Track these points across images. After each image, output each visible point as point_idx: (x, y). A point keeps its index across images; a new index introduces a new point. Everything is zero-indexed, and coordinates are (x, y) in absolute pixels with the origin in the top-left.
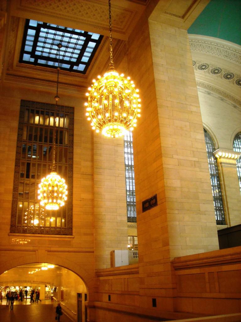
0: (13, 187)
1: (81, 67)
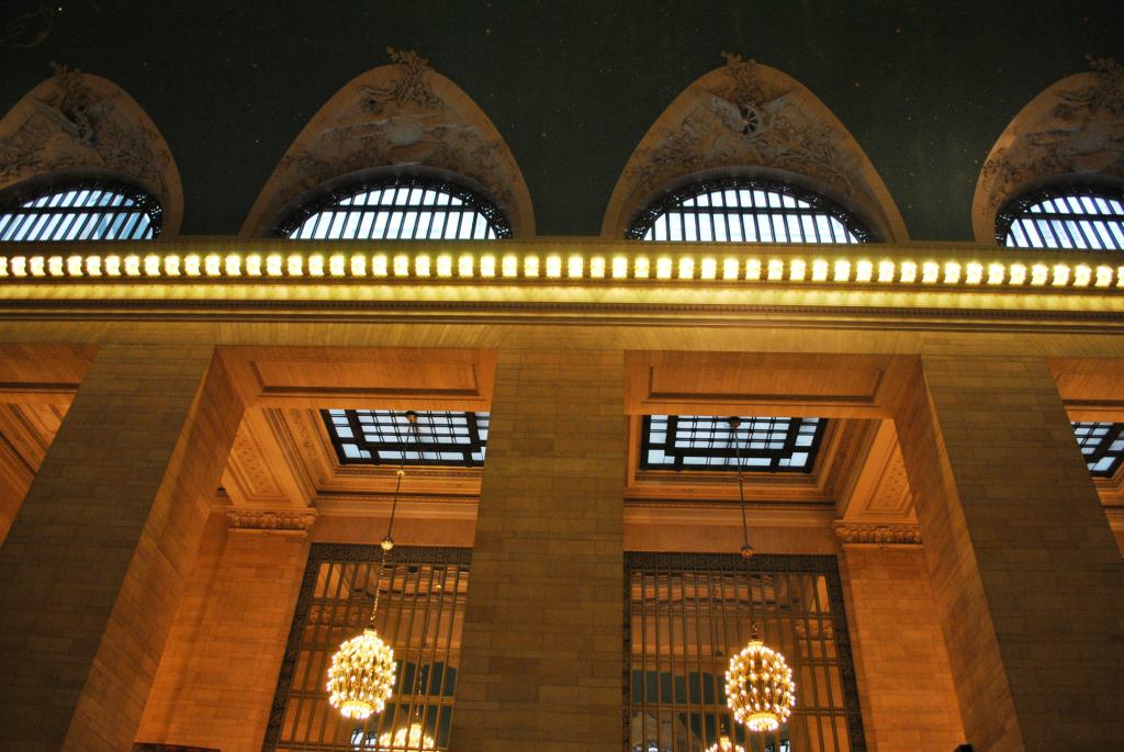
1: (799, 459)
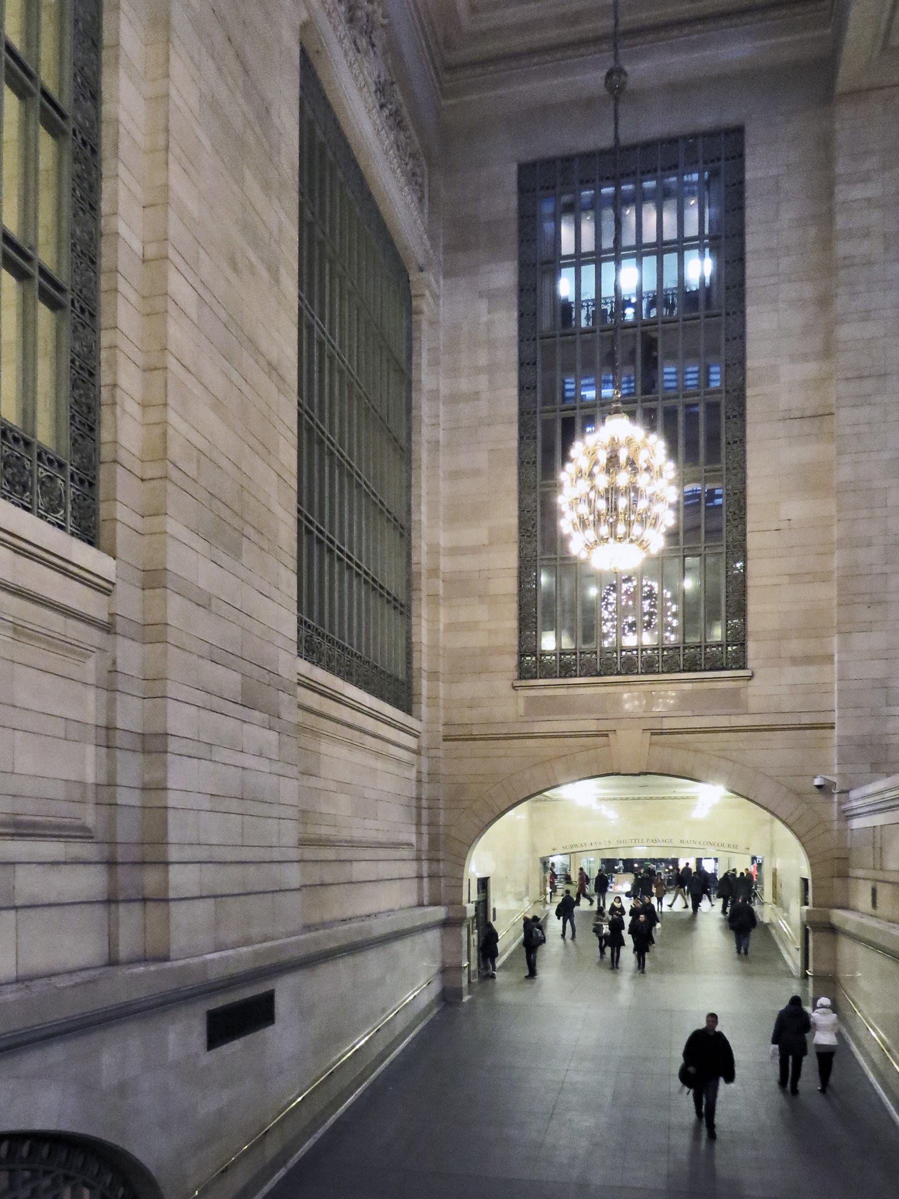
0: (520, 517)
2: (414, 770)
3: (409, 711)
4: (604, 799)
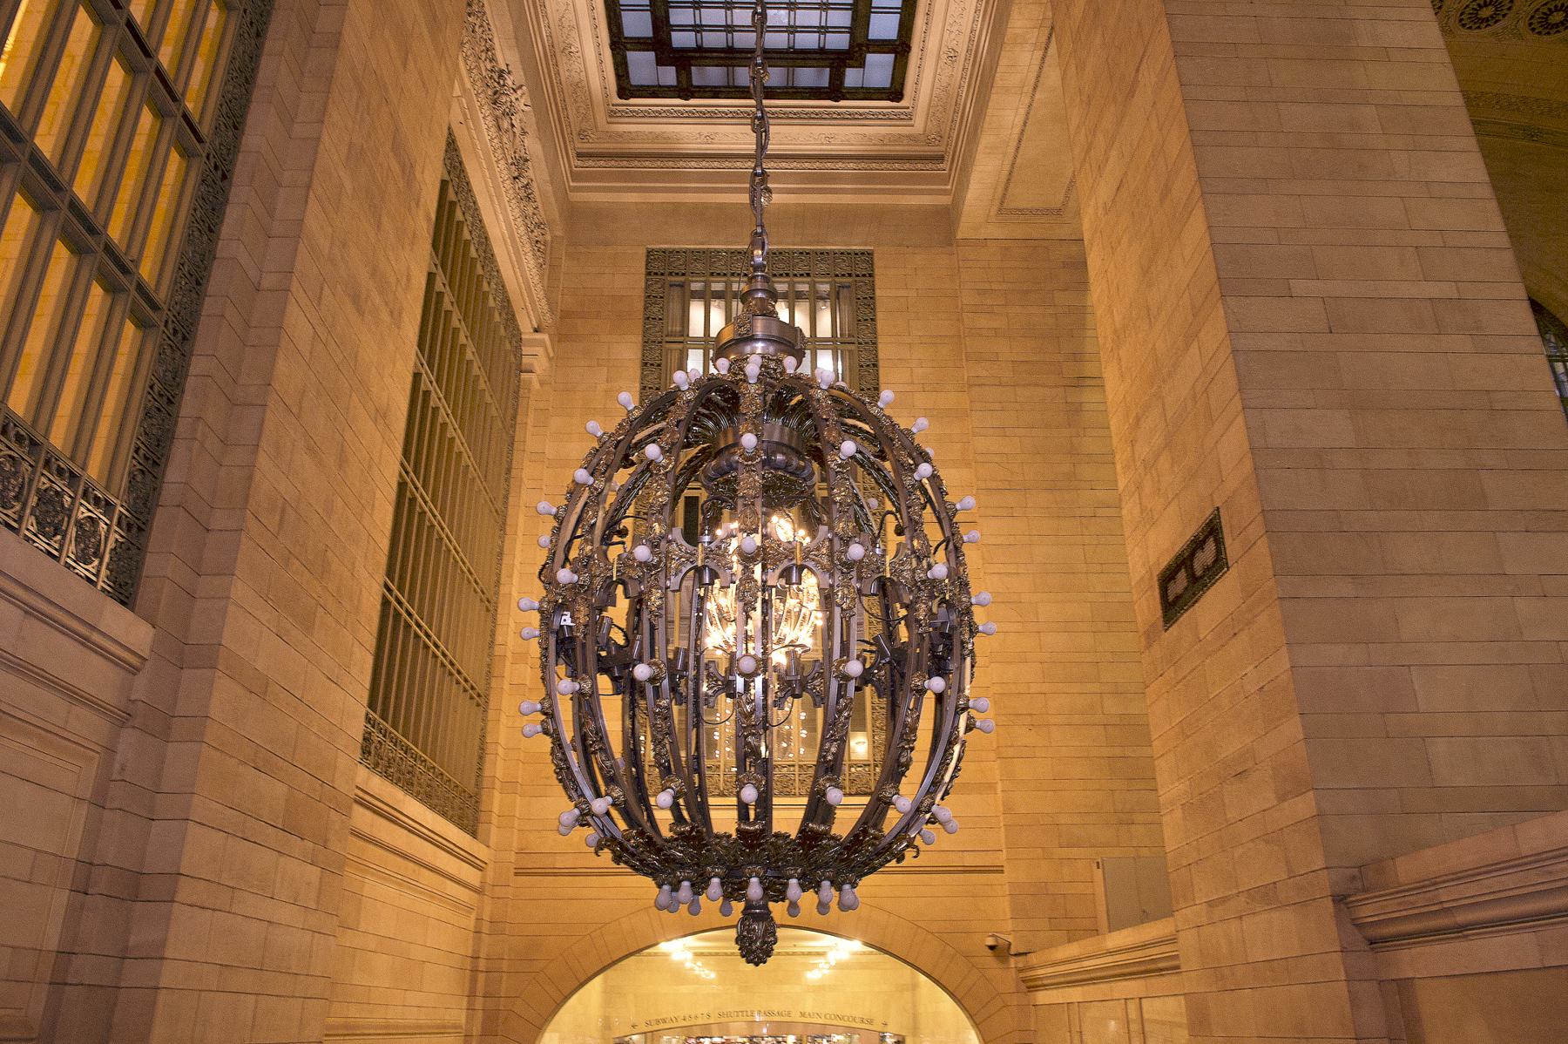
2: (473, 916)
3: (474, 834)
4: (702, 954)
